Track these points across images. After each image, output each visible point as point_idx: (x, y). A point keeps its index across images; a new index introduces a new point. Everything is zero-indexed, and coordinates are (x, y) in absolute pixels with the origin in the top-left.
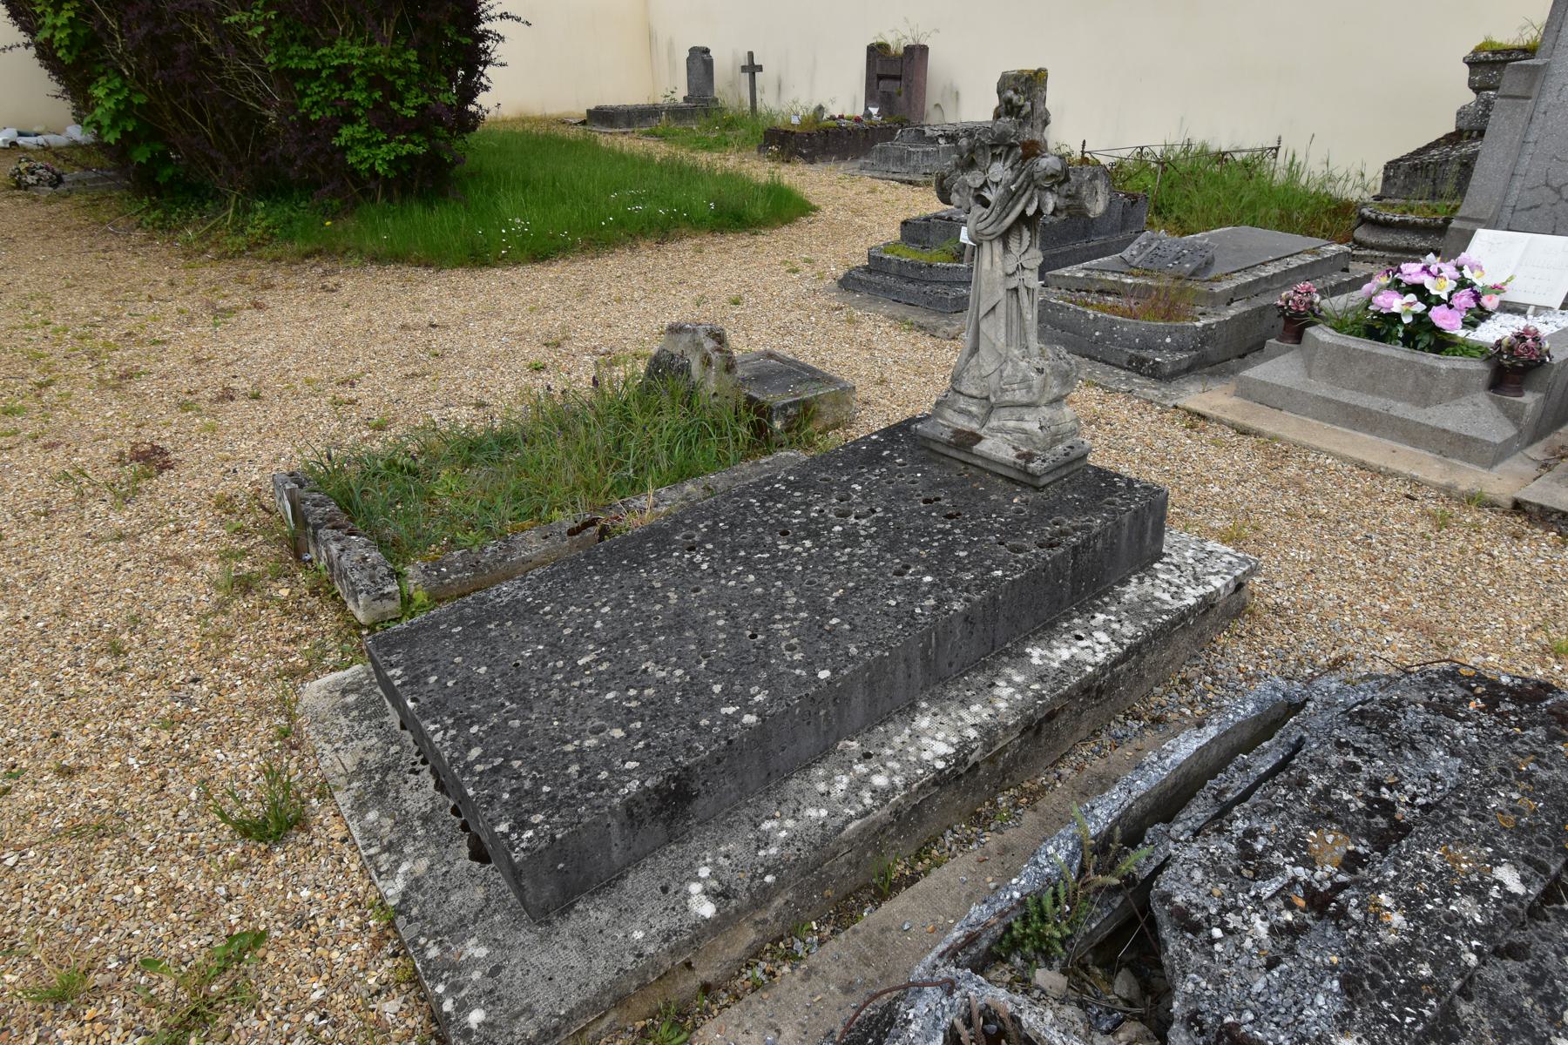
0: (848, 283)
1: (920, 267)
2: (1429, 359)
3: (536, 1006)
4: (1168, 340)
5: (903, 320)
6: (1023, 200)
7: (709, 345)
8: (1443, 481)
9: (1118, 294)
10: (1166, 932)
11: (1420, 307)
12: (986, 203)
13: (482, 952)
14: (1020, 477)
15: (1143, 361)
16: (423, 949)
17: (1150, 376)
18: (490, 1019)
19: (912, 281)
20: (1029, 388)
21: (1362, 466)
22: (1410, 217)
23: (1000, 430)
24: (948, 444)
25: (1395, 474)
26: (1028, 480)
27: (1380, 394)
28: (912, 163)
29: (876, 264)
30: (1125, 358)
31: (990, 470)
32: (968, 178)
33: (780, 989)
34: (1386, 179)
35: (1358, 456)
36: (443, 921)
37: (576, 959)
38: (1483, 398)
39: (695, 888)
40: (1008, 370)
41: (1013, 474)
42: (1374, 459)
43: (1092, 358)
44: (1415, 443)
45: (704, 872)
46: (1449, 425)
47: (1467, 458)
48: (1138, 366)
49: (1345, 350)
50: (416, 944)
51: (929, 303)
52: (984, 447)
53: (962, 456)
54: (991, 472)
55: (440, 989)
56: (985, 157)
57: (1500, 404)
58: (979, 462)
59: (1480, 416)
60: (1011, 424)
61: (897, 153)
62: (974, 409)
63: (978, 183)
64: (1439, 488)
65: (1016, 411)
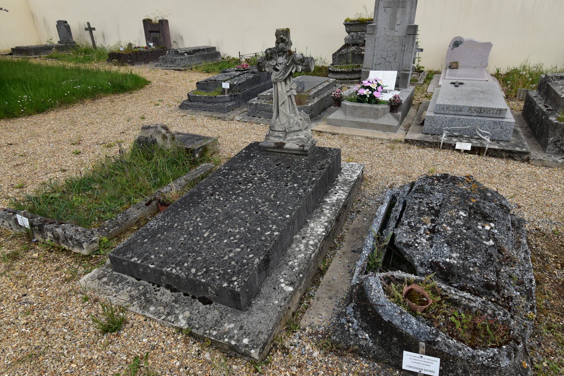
2: (376, 106)
3: (262, 331)
6: (291, 68)
7: (164, 131)
8: (388, 138)
10: (405, 250)
11: (370, 92)
12: (277, 70)
13: (232, 325)
14: (302, 152)
16: (210, 334)
18: (251, 339)
20: (299, 125)
21: (367, 138)
22: (343, 70)
23: (291, 140)
24: (274, 148)
25: (376, 138)
26: (304, 153)
27: (365, 118)
31: (291, 152)
32: (271, 63)
33: (314, 305)
35: (366, 135)
38: (389, 115)
39: (283, 285)
40: (292, 121)
44: (377, 129)
45: (282, 280)
46: (384, 123)
47: (390, 131)
49: (354, 106)
50: (206, 334)
52: (287, 145)
53: (279, 151)
54: (290, 153)
57: (394, 116)
58: (286, 151)
59: (389, 120)
60: (295, 137)
62: (281, 135)
63: (275, 64)
64: (387, 140)
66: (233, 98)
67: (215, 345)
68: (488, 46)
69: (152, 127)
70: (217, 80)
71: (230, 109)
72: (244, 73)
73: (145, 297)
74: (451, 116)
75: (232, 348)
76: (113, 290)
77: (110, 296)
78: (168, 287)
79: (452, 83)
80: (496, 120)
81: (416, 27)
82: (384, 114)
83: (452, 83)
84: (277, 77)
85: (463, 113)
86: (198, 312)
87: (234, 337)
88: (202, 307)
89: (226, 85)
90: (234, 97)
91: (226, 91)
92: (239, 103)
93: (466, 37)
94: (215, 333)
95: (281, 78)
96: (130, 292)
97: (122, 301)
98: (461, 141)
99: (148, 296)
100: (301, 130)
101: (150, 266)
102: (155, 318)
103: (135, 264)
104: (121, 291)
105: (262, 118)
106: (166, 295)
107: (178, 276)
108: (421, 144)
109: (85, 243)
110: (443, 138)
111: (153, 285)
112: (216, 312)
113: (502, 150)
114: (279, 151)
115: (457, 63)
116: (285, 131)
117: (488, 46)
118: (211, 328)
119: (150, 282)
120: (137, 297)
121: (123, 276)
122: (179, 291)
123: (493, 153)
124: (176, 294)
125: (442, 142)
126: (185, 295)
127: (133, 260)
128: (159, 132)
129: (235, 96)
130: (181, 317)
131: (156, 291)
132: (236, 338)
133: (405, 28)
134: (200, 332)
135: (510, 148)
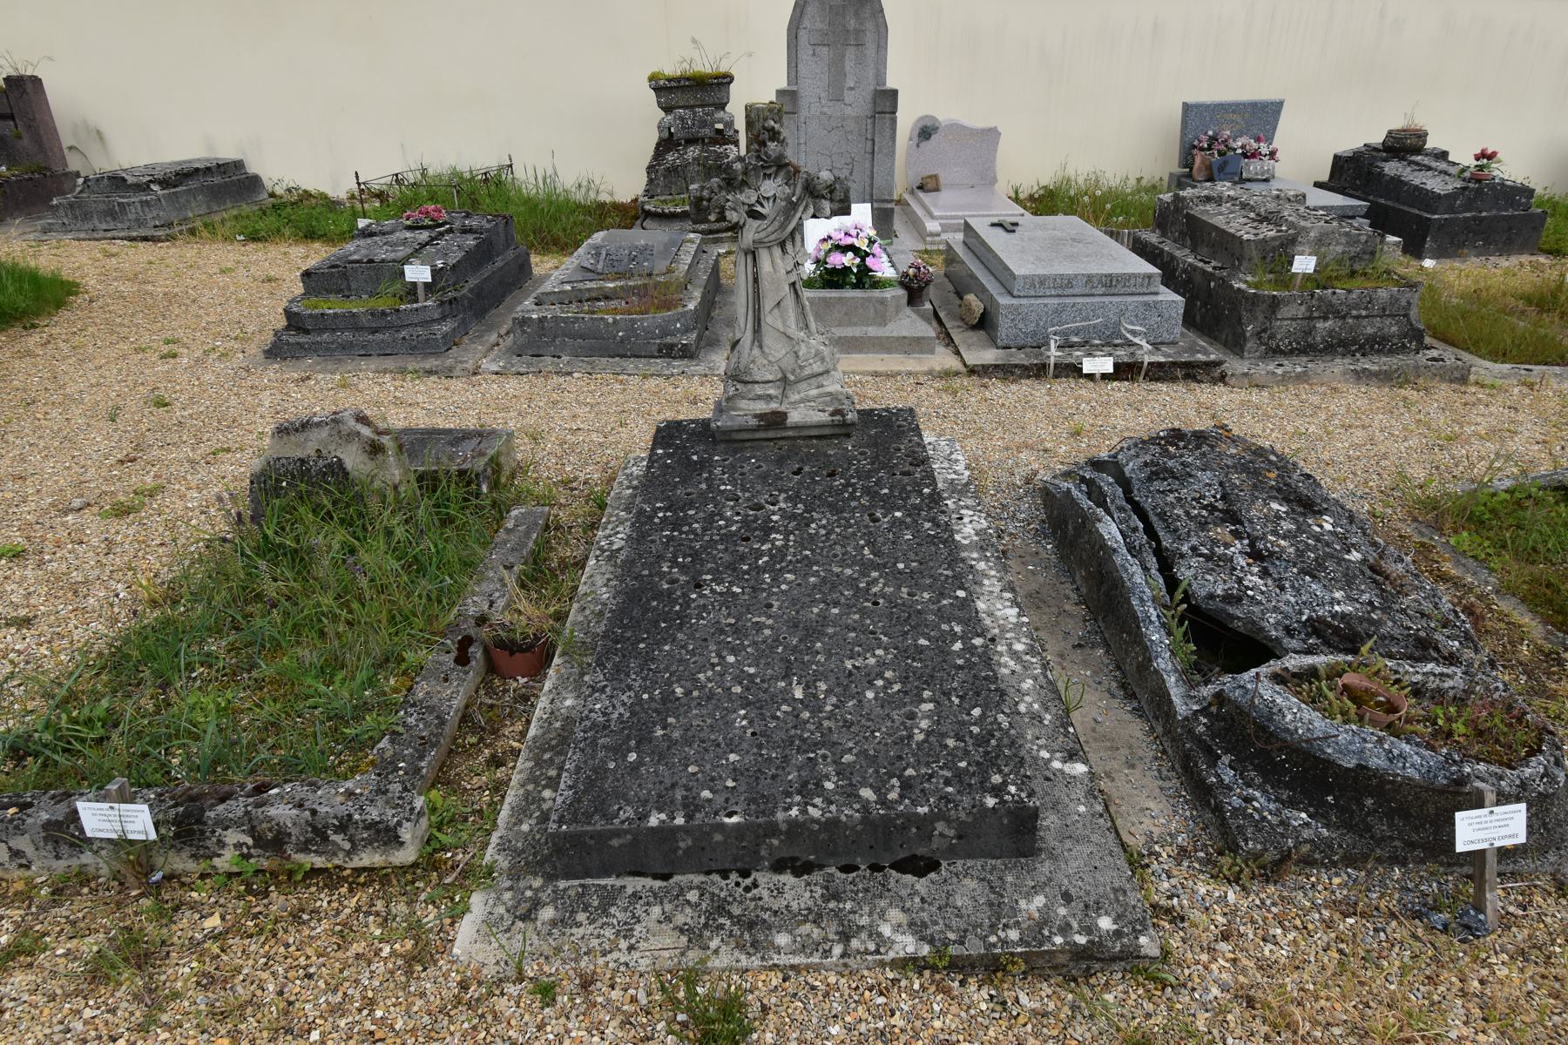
0: (276, 352)
1: (384, 314)
2: (876, 293)
3: (1116, 885)
5: (403, 371)
9: (607, 298)
13: (1039, 901)
14: (840, 429)
15: (671, 347)
16: (1005, 942)
18: (1114, 915)
19: (374, 331)
20: (823, 360)
21: (876, 374)
23: (802, 401)
24: (758, 429)
26: (843, 431)
27: (855, 324)
28: (132, 216)
29: (294, 321)
30: (654, 349)
31: (807, 434)
32: (742, 197)
35: (871, 369)
36: (984, 917)
37: (1086, 849)
38: (908, 311)
39: (1056, 765)
40: (803, 350)
41: (837, 431)
42: (881, 368)
43: (622, 356)
44: (889, 351)
45: (1045, 754)
46: (904, 333)
47: (921, 352)
48: (669, 352)
49: (824, 299)
50: (994, 945)
51: (413, 348)
52: (795, 417)
53: (771, 434)
55: (1058, 940)
56: (757, 177)
58: (790, 433)
59: (910, 324)
60: (814, 392)
61: (102, 207)
62: (771, 392)
64: (925, 374)
66: (447, 306)
67: (1037, 965)
68: (991, 135)
69: (318, 425)
70: (377, 258)
71: (451, 342)
72: (442, 234)
73: (730, 916)
74: (1056, 301)
75: (1080, 954)
76: (609, 933)
77: (615, 955)
78: (778, 867)
79: (993, 225)
80: (1146, 298)
81: (895, 93)
83: (993, 225)
84: (762, 235)
85: (1076, 291)
86: (923, 900)
87: (1069, 925)
88: (922, 885)
89: (418, 273)
90: (450, 307)
91: (421, 292)
92: (463, 321)
93: (943, 115)
94: (1014, 935)
95: (773, 237)
96: (668, 919)
97: (666, 954)
98: (1090, 355)
99: (736, 910)
100: (827, 372)
101: (727, 820)
102: (815, 959)
103: (666, 834)
104: (638, 928)
105: (565, 358)
106: (796, 892)
107: (832, 825)
108: (1006, 372)
109: (407, 825)
110: (1054, 354)
111: (725, 877)
112: (970, 883)
113: (1174, 364)
114: (771, 434)
115: (935, 177)
116: (784, 379)
117: (991, 135)
118: (993, 927)
119: (708, 873)
120: (706, 925)
121: (602, 882)
122: (821, 867)
123: (1159, 373)
124: (817, 876)
125: (1052, 360)
126: (847, 869)
127: (654, 821)
128: (353, 436)
129: (450, 302)
130: (886, 930)
131: (747, 889)
132: (1075, 925)
133: (869, 98)
134: (974, 948)
135: (1185, 358)
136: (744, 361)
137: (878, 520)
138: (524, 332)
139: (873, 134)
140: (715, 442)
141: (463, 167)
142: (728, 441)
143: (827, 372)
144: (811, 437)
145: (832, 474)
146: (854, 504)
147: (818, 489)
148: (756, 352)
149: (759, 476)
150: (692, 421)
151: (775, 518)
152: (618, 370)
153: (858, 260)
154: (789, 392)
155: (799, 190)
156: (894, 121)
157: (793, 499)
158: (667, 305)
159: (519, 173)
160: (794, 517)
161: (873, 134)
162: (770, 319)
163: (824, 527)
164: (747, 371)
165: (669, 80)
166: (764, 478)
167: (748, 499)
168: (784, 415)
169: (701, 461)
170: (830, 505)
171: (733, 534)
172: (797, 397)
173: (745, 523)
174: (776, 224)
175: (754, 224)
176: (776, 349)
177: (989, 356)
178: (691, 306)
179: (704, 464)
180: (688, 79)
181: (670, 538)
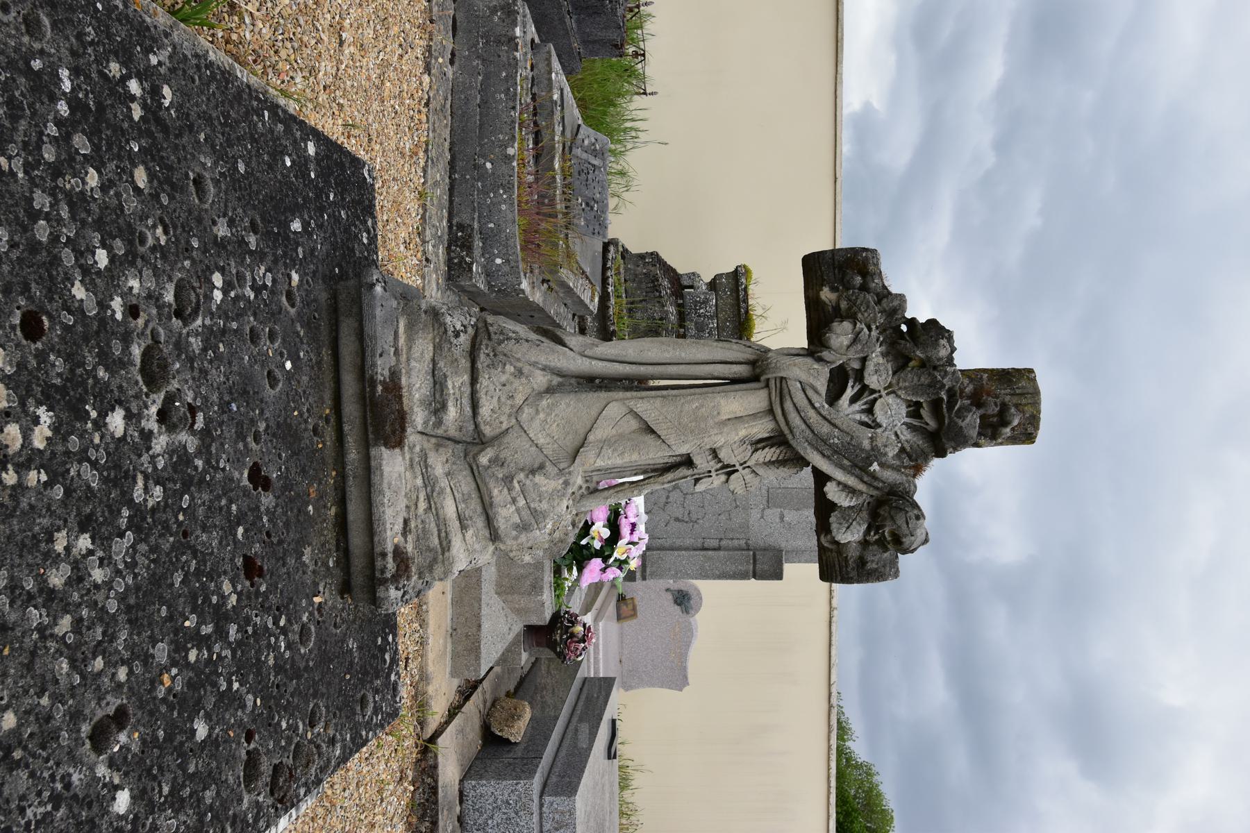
4: (499, 261)
6: (851, 481)
8: (431, 668)
11: (597, 545)
12: (833, 396)
15: (468, 248)
17: (449, 262)
20: (524, 527)
22: (613, 301)
25: (423, 623)
26: (358, 580)
30: (464, 217)
31: (353, 493)
32: (876, 356)
34: (642, 257)
38: (518, 627)
40: (547, 483)
41: (358, 563)
43: (452, 163)
46: (486, 626)
47: (455, 656)
53: (351, 409)
56: (914, 390)
57: (515, 643)
58: (353, 455)
60: (450, 509)
62: (452, 412)
63: (872, 380)
65: (475, 504)
81: (779, 576)
82: (518, 612)
93: (702, 619)
100: (494, 536)
105: (450, 71)
114: (351, 409)
116: (480, 441)
117: (678, 678)
133: (771, 541)
136: (520, 351)
137: (100, 738)
138: (494, 11)
139: (727, 549)
140: (331, 281)
141: (649, 27)
142: (334, 311)
143: (494, 536)
144: (342, 502)
145: (251, 569)
146: (161, 651)
147: (209, 540)
148: (541, 380)
149: (247, 378)
150: (373, 239)
151: (116, 422)
152: (433, 154)
153: (597, 545)
154: (447, 452)
155: (889, 476)
156: (743, 576)
157: (179, 471)
158: (529, 245)
159: (639, 101)
160: (118, 476)
161: (727, 549)
162: (615, 411)
163: (78, 577)
164: (499, 360)
165: (746, 290)
166: (245, 391)
167: (180, 345)
168: (396, 439)
169: (286, 239)
170: (158, 581)
171: (56, 287)
172: (439, 469)
173: (101, 329)
174: (825, 429)
175: (822, 385)
176: (552, 423)
177: (449, 772)
178: (525, 285)
179: (280, 248)
180: (747, 312)
181: (44, 86)
